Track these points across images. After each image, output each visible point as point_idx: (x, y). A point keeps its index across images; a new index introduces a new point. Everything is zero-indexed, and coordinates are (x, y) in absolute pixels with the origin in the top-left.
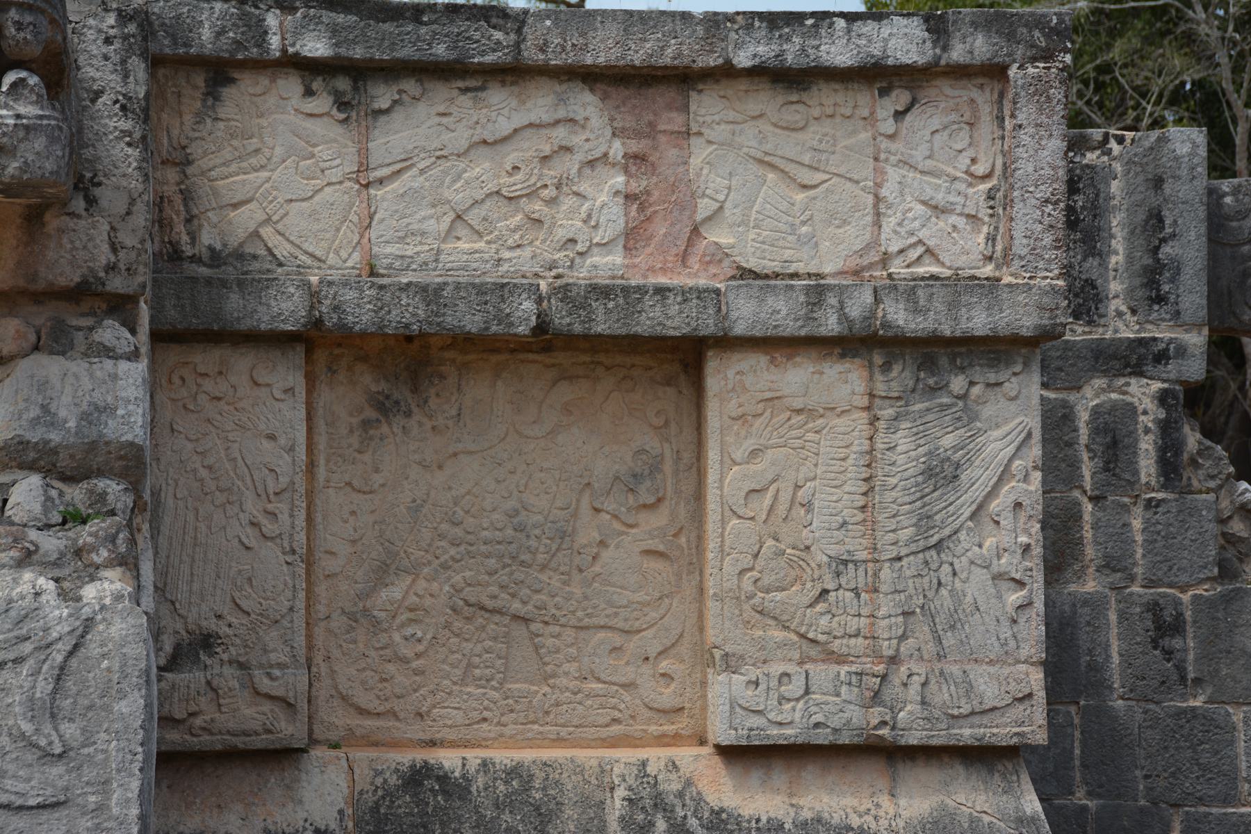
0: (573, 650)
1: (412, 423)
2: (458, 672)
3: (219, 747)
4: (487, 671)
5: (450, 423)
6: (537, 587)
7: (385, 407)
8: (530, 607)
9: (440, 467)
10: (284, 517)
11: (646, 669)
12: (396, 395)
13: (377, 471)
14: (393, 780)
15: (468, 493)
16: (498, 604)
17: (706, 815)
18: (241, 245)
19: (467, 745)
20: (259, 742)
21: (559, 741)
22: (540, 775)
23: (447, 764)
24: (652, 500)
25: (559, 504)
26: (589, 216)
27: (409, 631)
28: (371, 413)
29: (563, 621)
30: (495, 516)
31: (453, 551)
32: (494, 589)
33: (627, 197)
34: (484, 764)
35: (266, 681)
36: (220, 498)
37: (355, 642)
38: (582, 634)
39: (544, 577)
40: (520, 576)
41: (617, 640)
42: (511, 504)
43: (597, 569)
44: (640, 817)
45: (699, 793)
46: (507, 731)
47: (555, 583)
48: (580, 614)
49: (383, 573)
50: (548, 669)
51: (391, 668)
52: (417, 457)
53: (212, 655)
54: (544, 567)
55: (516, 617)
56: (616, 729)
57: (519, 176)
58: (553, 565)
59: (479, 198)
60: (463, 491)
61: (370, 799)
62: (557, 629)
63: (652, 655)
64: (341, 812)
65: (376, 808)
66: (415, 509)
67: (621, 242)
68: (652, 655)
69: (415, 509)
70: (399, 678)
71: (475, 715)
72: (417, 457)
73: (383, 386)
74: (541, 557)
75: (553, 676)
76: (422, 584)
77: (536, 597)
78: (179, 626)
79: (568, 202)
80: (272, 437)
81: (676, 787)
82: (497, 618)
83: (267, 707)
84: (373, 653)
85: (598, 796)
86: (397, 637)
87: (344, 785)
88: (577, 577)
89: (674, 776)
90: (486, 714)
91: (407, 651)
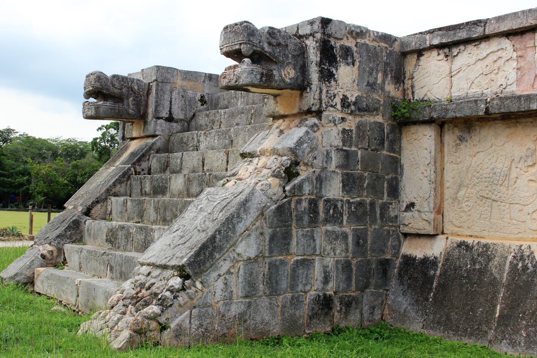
0: (508, 211)
1: (468, 144)
2: (479, 216)
3: (414, 233)
4: (486, 216)
5: (477, 143)
6: (499, 191)
7: (461, 139)
8: (497, 197)
9: (475, 156)
10: (429, 171)
11: (529, 217)
12: (464, 136)
13: (459, 158)
14: (455, 245)
15: (481, 163)
16: (488, 196)
17: (534, 263)
18: (423, 98)
19: (477, 237)
20: (422, 232)
21: (504, 238)
22: (492, 247)
23: (469, 242)
24: (531, 164)
25: (505, 166)
26: (506, 77)
27: (467, 203)
28: (458, 142)
29: (506, 201)
30: (487, 170)
31: (477, 180)
32: (487, 192)
33: (517, 69)
34: (478, 243)
35: (424, 216)
36: (416, 166)
37: (454, 206)
38: (511, 205)
39: (501, 188)
40: (494, 188)
41: (520, 207)
42: (492, 166)
43: (515, 186)
44: (515, 262)
45: (534, 256)
46: (491, 234)
47: (504, 190)
48: (510, 199)
49: (460, 186)
50: (502, 216)
51: (462, 214)
52: (469, 153)
53: (413, 208)
54: (501, 185)
55: (494, 200)
56: (520, 235)
57: (488, 68)
58: (504, 184)
59: (477, 76)
60: (479, 163)
61: (449, 250)
62: (504, 204)
63: (530, 213)
64: (441, 253)
65: (448, 253)
66: (468, 169)
67: (515, 83)
68: (530, 213)
69: (468, 169)
70: (464, 217)
71: (482, 229)
72: (469, 153)
73: (461, 134)
74: (500, 182)
75: (503, 218)
76: (469, 190)
77: (499, 194)
78: (407, 200)
79: (501, 73)
80: (426, 149)
81: (528, 254)
82: (488, 200)
83: (425, 222)
84: (458, 210)
85: (506, 255)
86: (464, 205)
87: (444, 245)
88: (510, 188)
89: (528, 250)
90: (485, 228)
91: (467, 210)
